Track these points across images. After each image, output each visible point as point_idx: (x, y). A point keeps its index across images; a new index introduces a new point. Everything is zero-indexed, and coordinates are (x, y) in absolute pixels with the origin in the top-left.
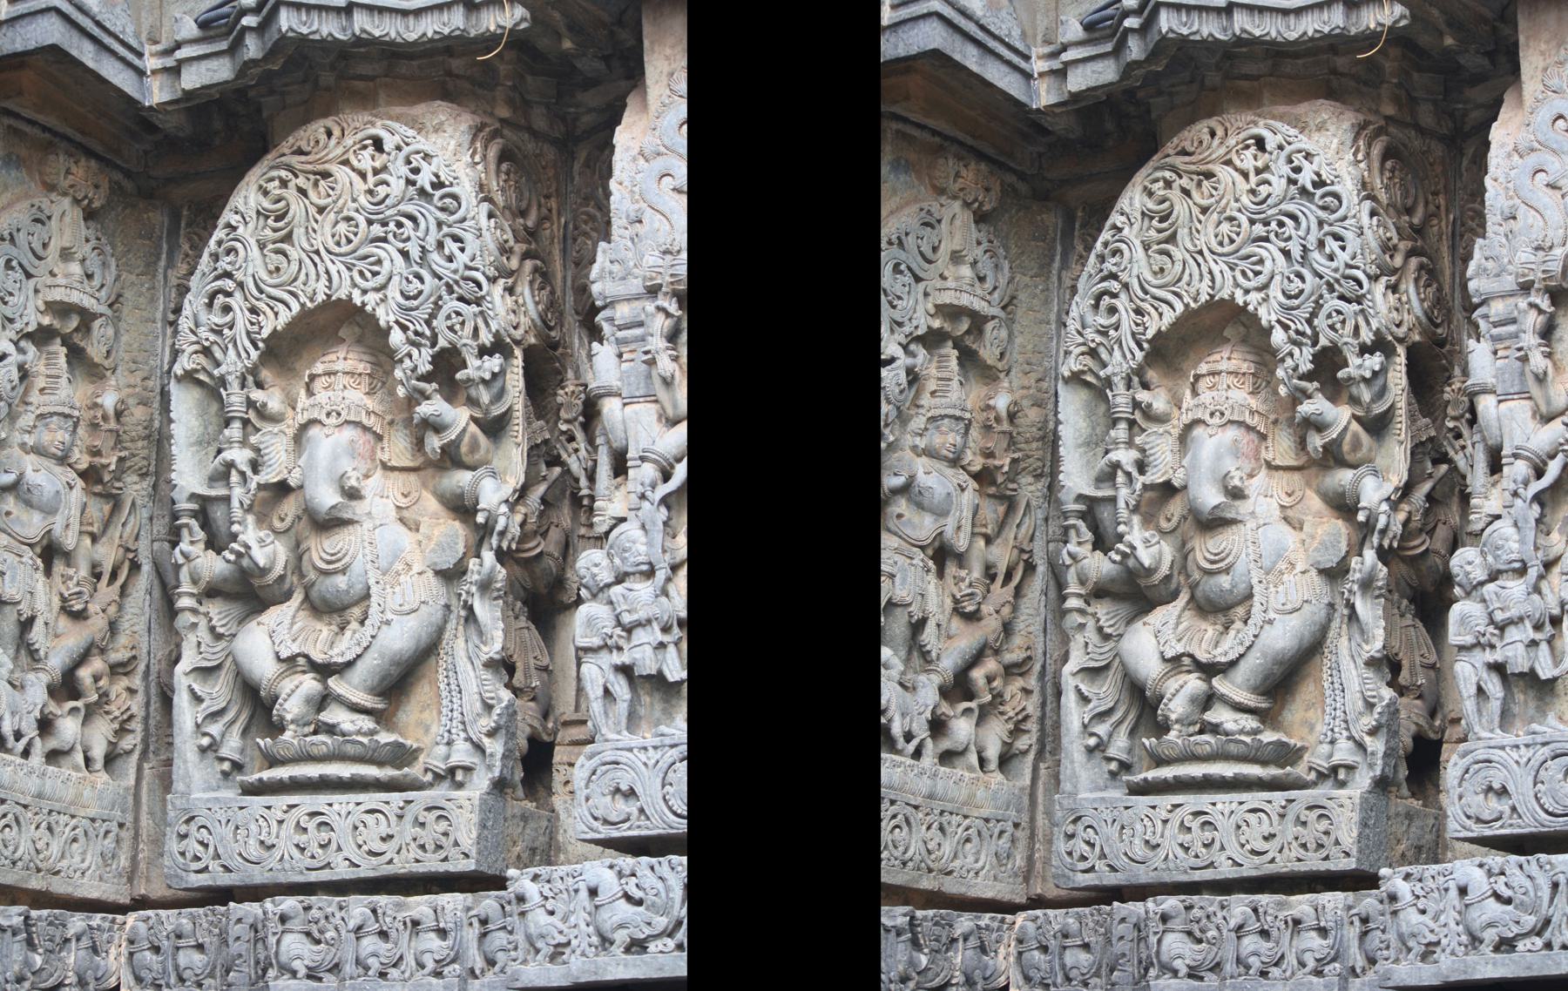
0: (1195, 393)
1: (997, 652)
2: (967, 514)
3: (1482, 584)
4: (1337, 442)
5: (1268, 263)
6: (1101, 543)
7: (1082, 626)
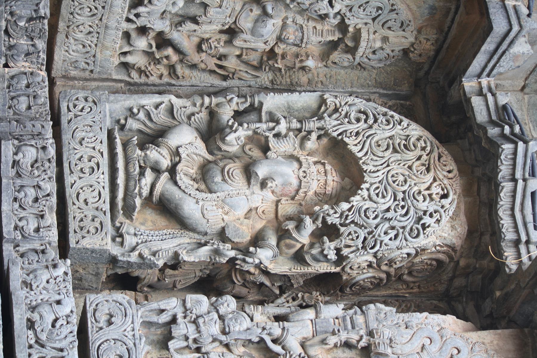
0: (315, 163)
1: (181, 61)
2: (253, 45)
3: (217, 312)
4: (291, 237)
5: (383, 201)
6: (238, 115)
7: (195, 105)
